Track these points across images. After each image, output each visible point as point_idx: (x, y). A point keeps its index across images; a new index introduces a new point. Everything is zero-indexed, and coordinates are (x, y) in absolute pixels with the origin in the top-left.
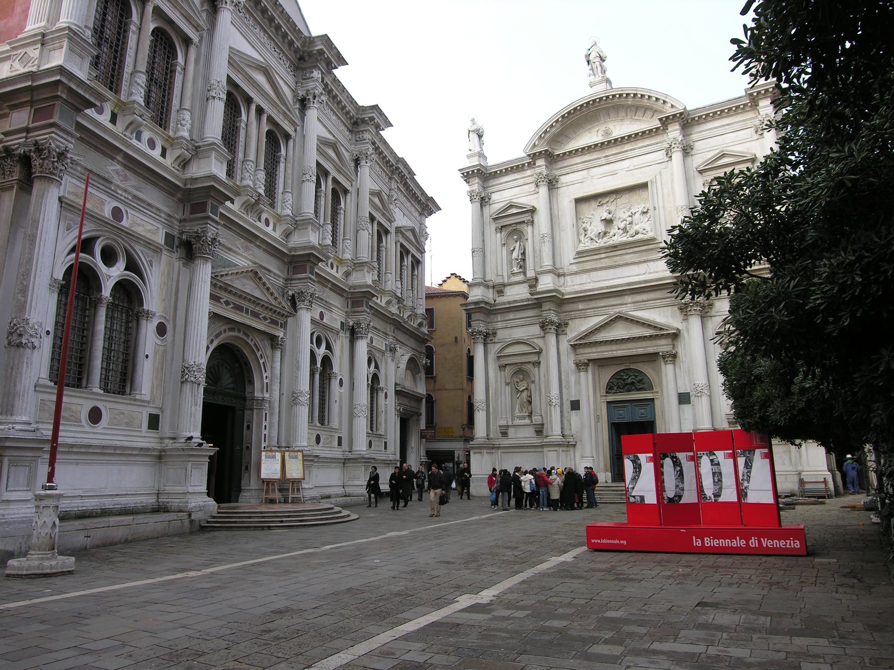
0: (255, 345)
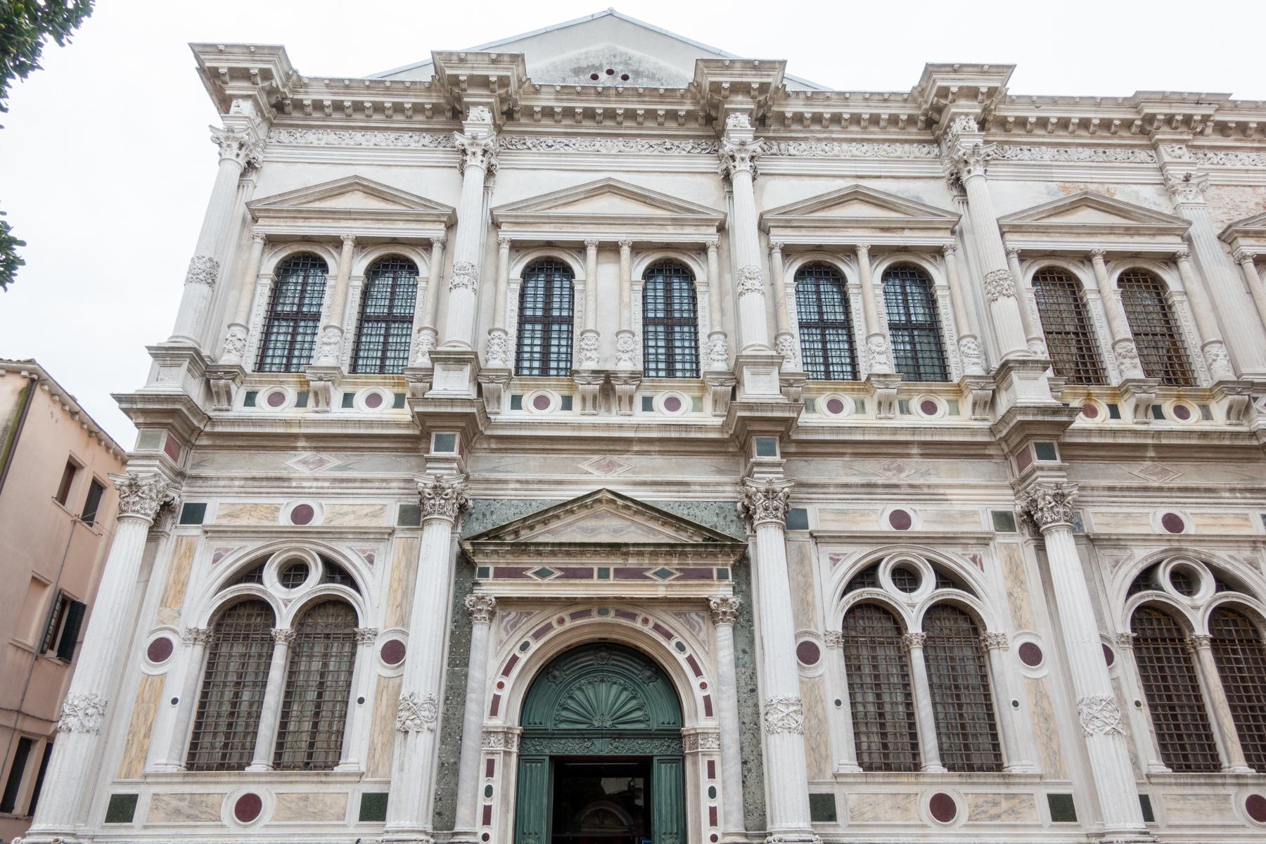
0: (657, 627)
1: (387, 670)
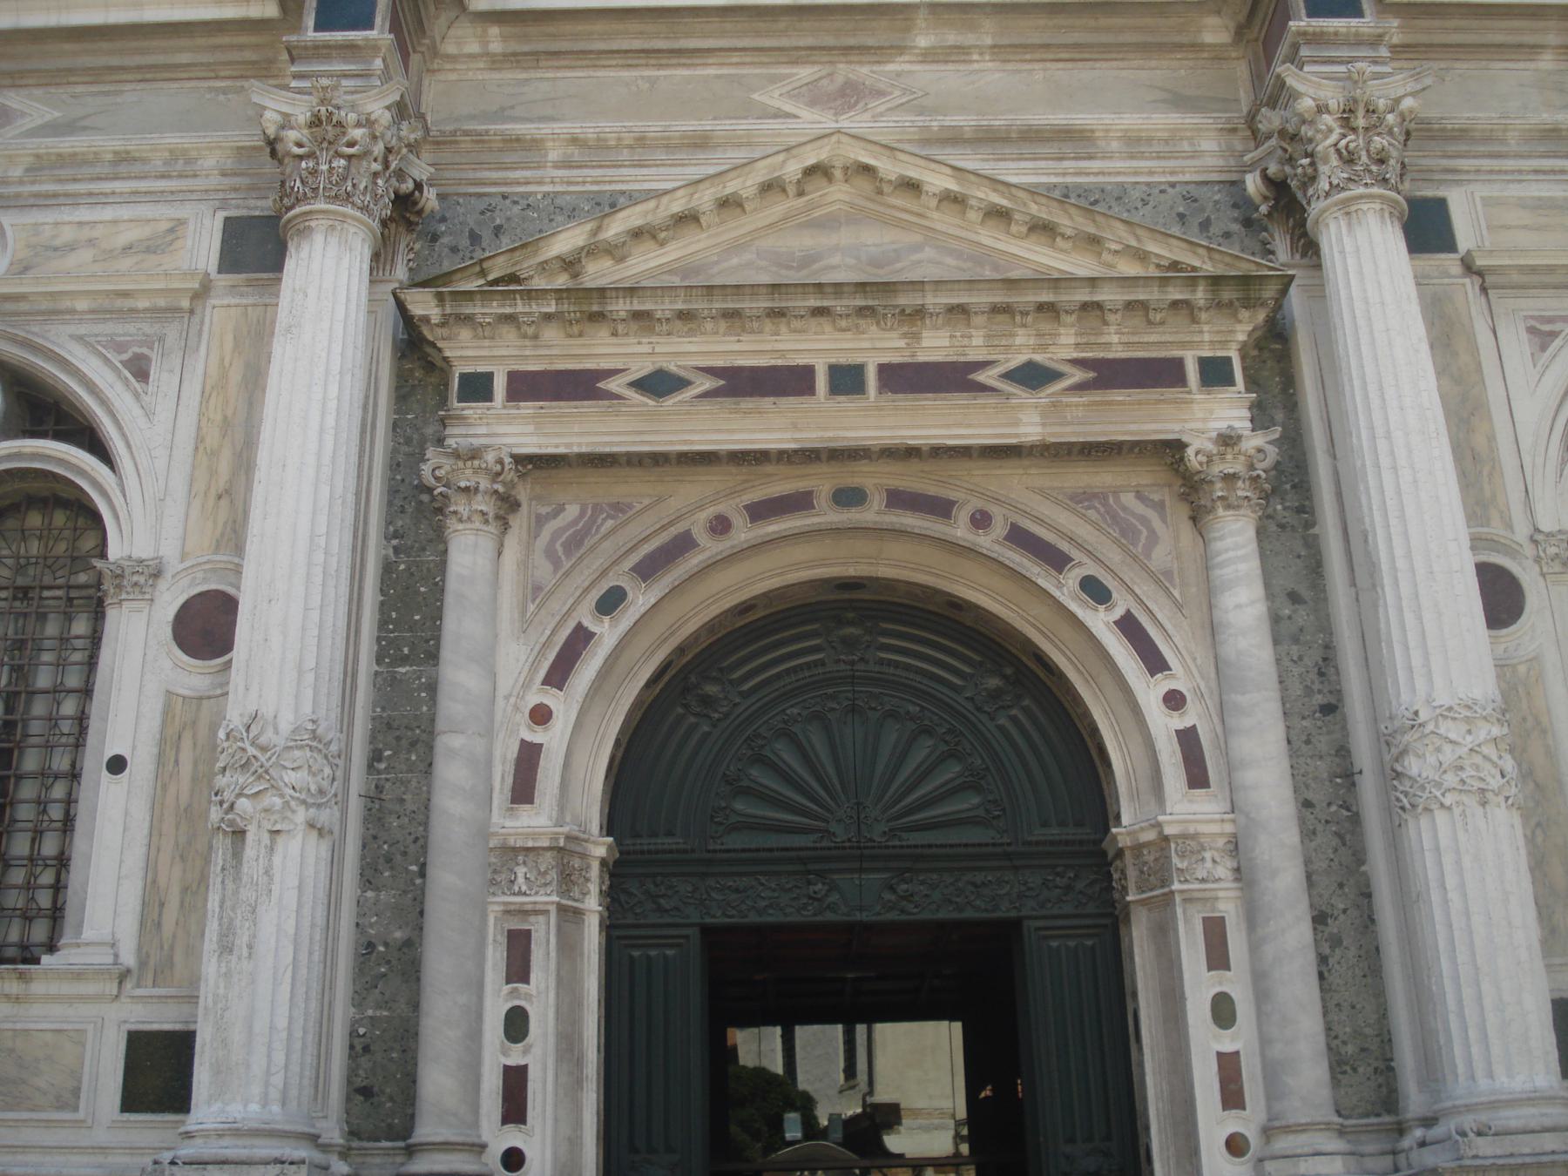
0: (1019, 537)
1: (191, 675)
